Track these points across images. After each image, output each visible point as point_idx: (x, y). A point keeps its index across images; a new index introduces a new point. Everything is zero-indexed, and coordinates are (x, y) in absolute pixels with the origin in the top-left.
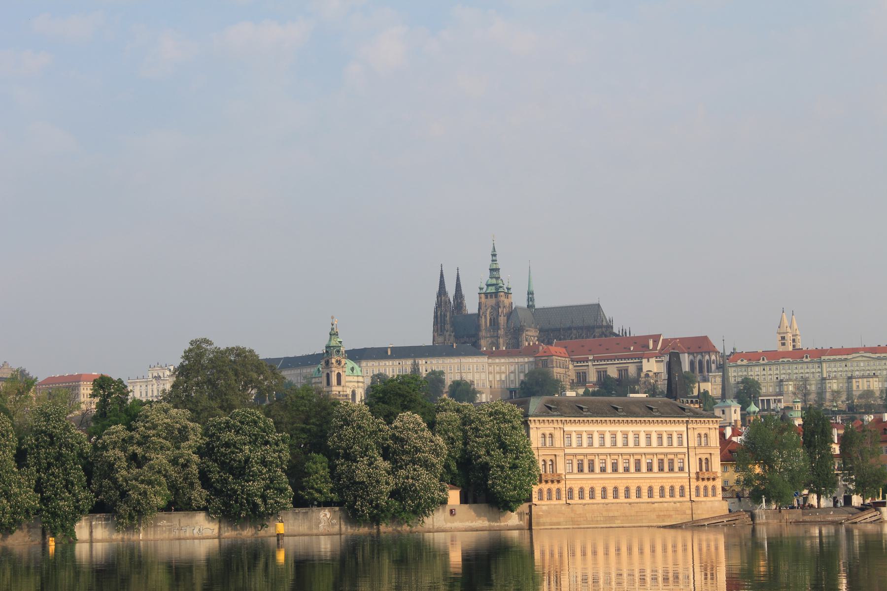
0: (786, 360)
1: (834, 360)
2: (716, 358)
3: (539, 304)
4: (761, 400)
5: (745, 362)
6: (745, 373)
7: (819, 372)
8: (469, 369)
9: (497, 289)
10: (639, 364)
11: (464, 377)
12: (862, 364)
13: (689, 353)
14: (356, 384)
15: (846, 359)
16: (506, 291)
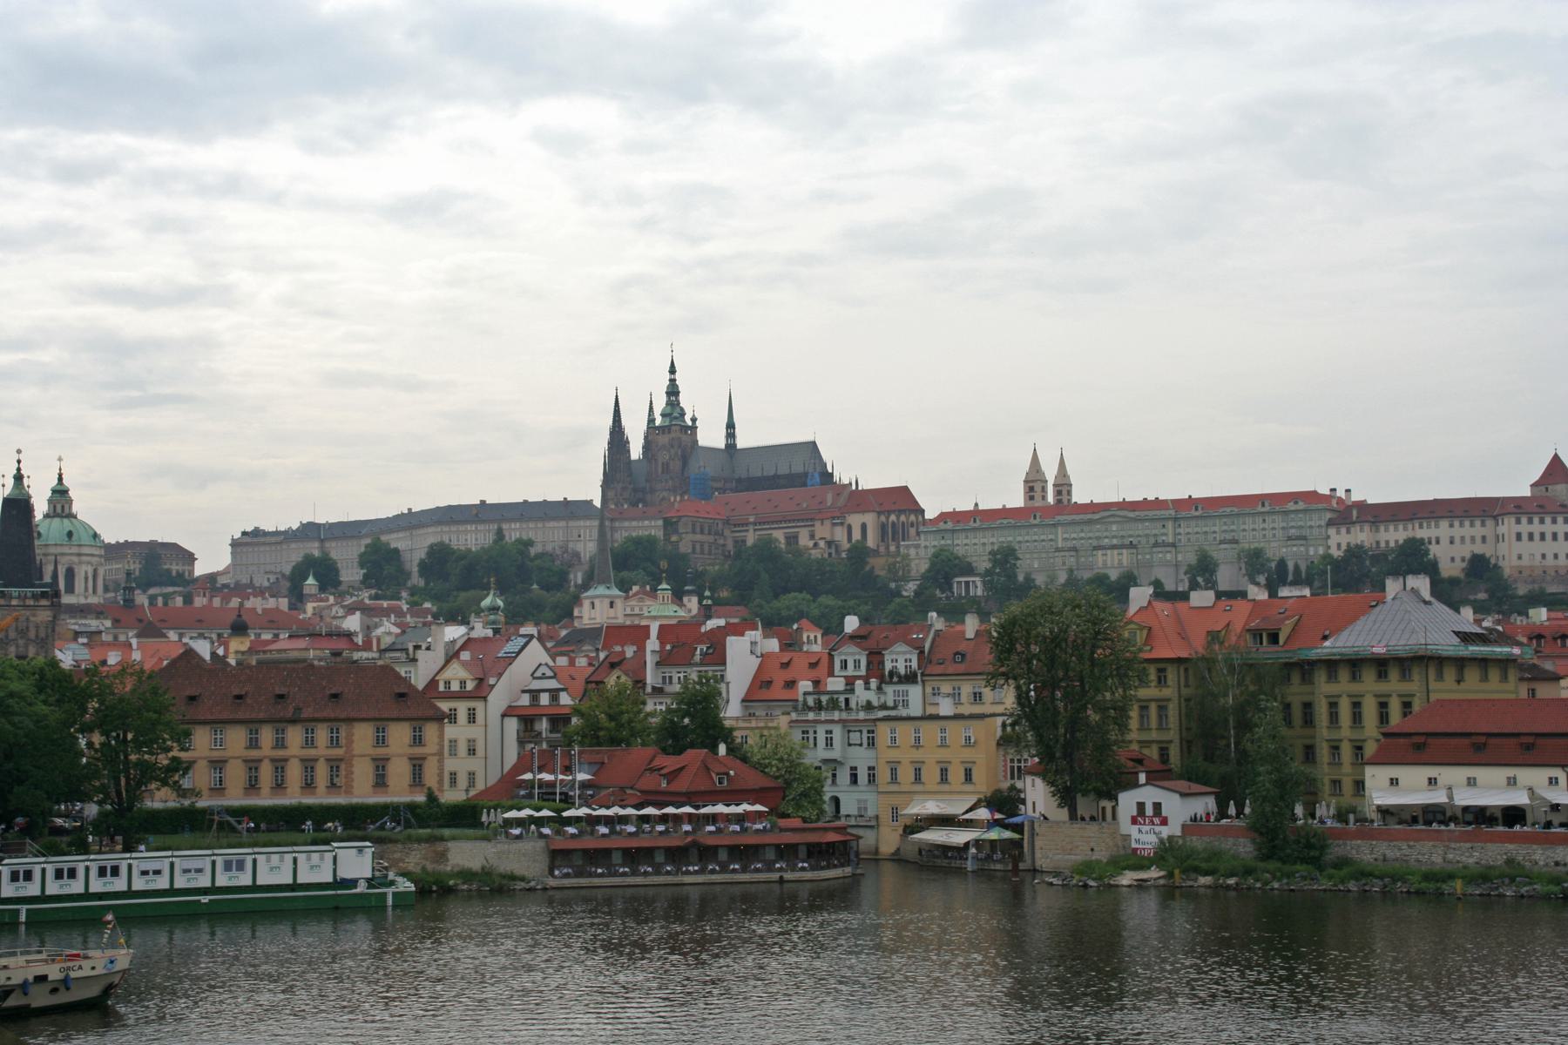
0: (1005, 521)
1: (1073, 523)
2: (917, 519)
3: (741, 443)
4: (958, 582)
5: (950, 525)
6: (949, 542)
7: (1051, 540)
8: (580, 536)
9: (671, 421)
10: (810, 529)
11: (571, 545)
12: (1114, 528)
13: (879, 513)
14: (75, 559)
15: (1090, 522)
16: (690, 423)
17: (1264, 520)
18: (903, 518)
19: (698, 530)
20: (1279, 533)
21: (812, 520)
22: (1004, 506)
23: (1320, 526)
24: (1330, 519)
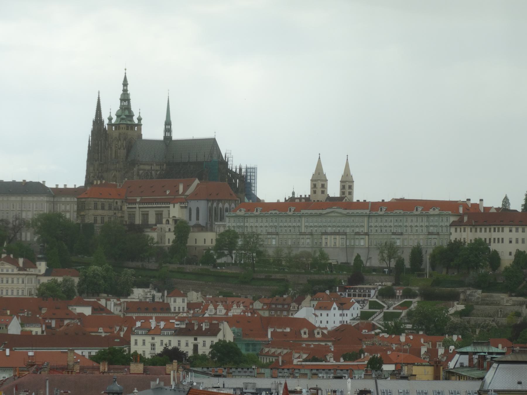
0: (274, 212)
1: (311, 215)
2: (230, 206)
3: (176, 136)
6: (242, 224)
7: (299, 226)
13: (208, 200)
15: (321, 215)
17: (412, 220)
18: (220, 205)
19: (99, 206)
20: (425, 229)
21: (170, 203)
22: (278, 200)
23: (446, 226)
24: (453, 221)
